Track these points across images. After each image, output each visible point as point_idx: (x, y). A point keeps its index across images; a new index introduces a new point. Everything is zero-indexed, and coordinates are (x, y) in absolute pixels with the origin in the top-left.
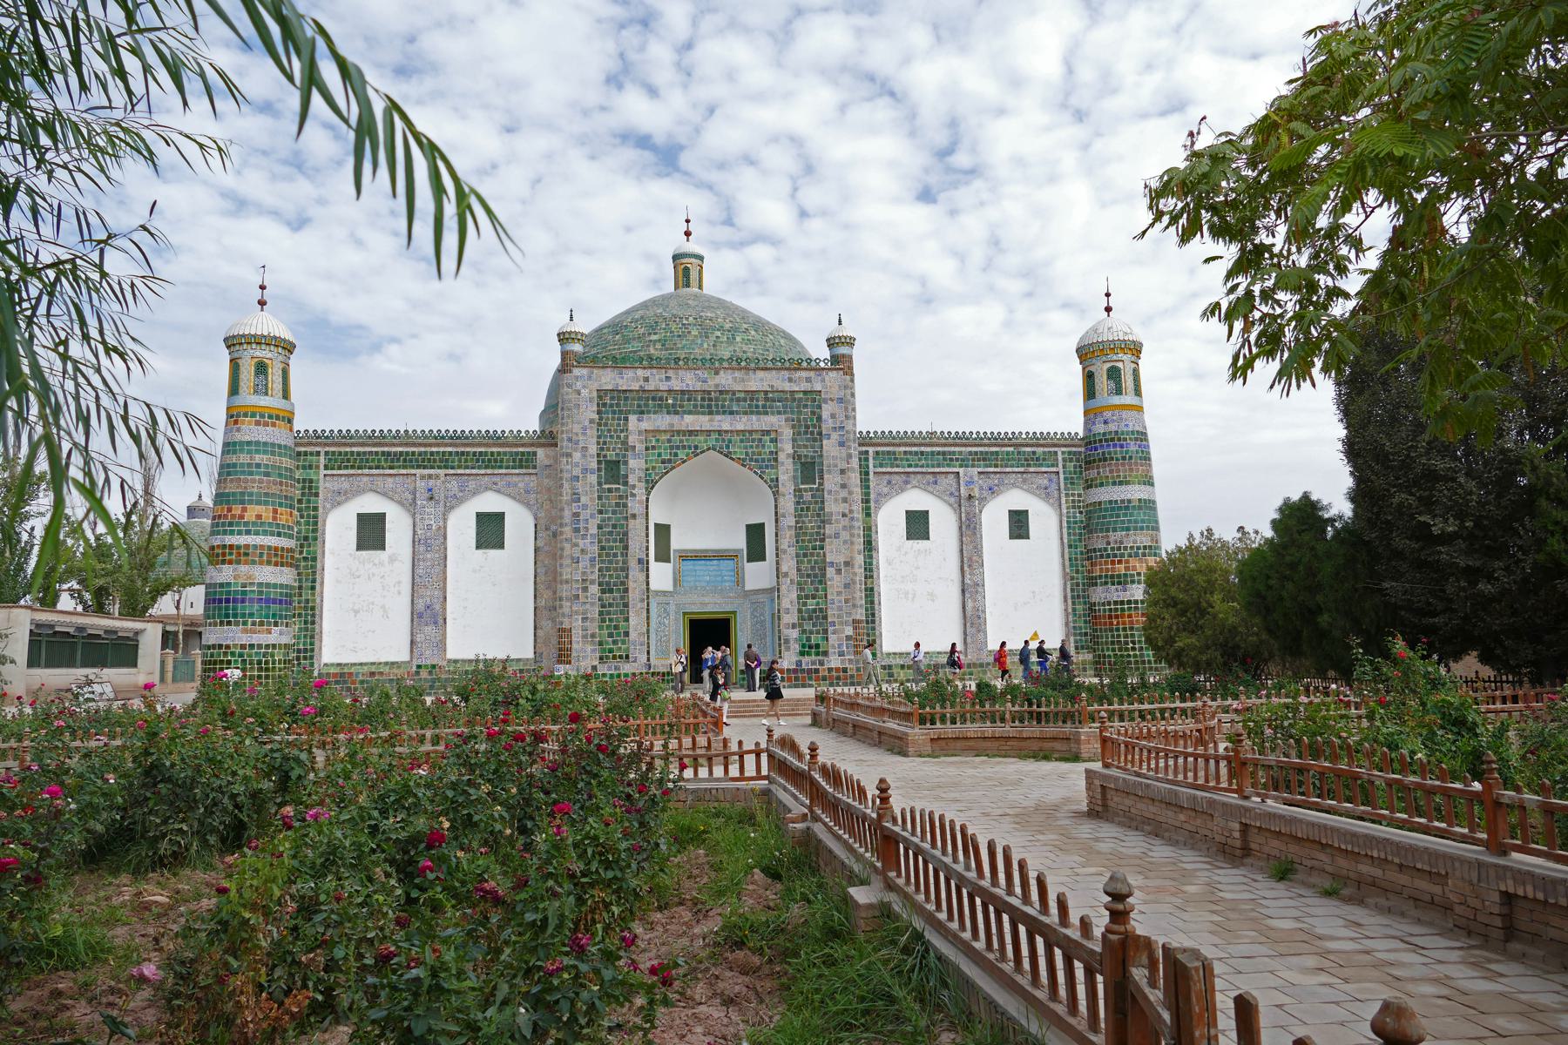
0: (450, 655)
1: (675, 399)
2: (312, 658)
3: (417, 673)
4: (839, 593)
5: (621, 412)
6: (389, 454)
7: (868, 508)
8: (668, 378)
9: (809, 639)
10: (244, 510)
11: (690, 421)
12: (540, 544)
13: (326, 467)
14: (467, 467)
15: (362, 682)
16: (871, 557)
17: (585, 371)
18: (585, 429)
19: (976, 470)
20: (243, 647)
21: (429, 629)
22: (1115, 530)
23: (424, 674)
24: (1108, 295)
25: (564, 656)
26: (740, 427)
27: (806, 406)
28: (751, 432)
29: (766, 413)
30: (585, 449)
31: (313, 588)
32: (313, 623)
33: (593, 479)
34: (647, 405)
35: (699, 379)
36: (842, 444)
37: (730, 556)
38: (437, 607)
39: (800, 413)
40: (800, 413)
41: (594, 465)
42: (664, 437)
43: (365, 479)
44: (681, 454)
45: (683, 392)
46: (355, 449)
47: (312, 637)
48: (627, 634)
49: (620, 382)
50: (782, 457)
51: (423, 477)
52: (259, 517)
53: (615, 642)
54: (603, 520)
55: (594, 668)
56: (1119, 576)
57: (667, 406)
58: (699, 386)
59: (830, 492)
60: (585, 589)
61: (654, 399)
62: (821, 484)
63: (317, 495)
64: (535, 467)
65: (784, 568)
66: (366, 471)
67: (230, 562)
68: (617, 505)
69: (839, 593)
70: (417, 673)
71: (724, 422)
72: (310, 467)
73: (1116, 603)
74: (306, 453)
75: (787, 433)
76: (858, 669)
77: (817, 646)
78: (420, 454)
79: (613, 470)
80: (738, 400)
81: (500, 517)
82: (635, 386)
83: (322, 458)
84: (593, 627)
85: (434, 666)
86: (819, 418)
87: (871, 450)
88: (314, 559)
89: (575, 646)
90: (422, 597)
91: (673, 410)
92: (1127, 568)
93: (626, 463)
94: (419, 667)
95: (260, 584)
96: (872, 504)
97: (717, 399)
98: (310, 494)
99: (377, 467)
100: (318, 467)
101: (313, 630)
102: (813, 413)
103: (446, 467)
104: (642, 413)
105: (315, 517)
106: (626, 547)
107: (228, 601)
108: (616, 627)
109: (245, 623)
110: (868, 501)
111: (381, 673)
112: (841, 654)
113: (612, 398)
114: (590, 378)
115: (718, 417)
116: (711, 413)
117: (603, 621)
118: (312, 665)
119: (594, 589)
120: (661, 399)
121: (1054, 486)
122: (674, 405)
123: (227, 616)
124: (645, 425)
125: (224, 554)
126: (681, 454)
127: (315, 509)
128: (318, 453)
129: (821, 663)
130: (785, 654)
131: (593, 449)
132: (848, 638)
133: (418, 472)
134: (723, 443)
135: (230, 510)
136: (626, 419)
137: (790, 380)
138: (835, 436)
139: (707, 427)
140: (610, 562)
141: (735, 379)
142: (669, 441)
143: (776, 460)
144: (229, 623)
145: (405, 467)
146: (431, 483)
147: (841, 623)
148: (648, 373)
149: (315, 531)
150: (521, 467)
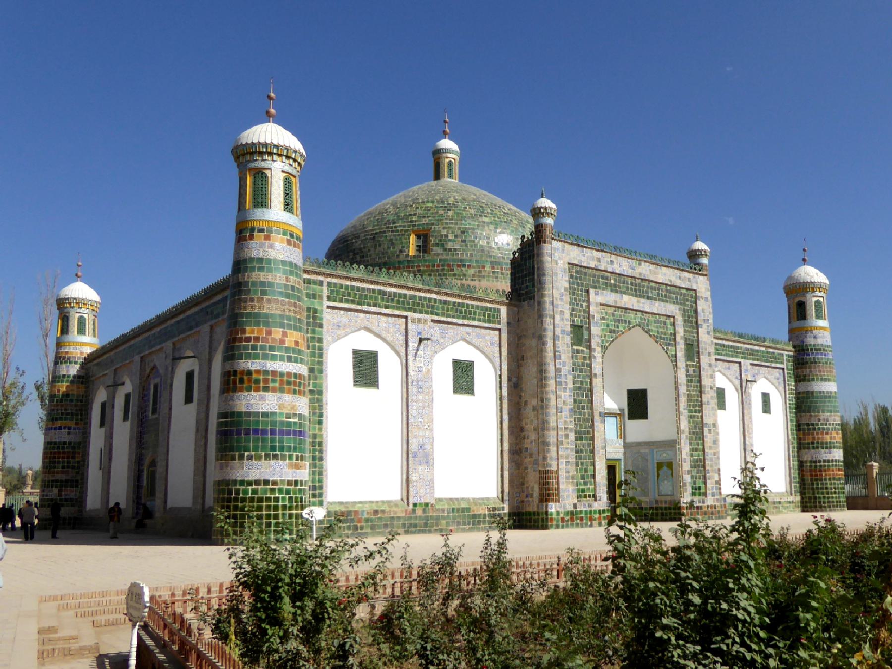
0: (438, 494)
3: (414, 511)
6: (384, 293)
10: (285, 334)
15: (367, 520)
19: (751, 362)
22: (823, 411)
23: (419, 512)
25: (547, 494)
38: (428, 447)
44: (621, 328)
51: (413, 321)
52: (297, 343)
53: (585, 483)
55: (575, 506)
56: (826, 443)
60: (567, 436)
66: (365, 308)
70: (414, 511)
73: (824, 461)
78: (411, 297)
79: (580, 334)
84: (572, 469)
85: (427, 504)
90: (416, 437)
92: (831, 438)
94: (415, 505)
99: (375, 305)
103: (432, 313)
107: (273, 432)
109: (290, 457)
111: (383, 512)
113: (577, 272)
117: (577, 465)
119: (572, 436)
133: (410, 314)
140: (580, 414)
145: (398, 308)
146: (421, 326)
148: (600, 254)
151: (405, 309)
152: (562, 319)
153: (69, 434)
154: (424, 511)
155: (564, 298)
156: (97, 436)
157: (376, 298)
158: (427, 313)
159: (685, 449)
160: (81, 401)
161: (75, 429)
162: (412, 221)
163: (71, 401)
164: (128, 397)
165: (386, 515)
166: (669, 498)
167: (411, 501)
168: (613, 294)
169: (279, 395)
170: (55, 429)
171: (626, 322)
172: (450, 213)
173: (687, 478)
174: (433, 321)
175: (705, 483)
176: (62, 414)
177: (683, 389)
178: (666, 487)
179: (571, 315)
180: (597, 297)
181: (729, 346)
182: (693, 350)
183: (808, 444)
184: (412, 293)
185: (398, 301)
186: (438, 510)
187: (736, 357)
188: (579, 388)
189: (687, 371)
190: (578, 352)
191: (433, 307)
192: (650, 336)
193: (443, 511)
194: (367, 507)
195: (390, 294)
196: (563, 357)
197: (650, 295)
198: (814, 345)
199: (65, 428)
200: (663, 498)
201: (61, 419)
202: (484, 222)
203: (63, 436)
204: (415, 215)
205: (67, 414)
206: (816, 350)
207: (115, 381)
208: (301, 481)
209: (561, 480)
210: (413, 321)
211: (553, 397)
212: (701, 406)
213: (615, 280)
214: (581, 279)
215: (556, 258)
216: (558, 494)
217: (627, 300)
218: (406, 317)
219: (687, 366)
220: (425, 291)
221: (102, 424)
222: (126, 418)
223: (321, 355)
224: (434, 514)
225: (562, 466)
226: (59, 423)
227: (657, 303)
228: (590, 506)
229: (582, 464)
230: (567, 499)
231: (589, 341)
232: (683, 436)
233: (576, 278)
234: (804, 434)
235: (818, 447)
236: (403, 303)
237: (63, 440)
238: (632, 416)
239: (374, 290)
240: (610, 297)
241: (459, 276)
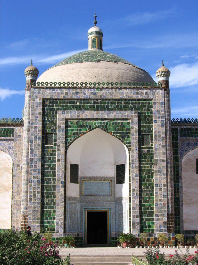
1: (80, 103)
5: (54, 109)
7: (177, 157)
8: (77, 93)
11: (88, 114)
12: (15, 174)
16: (178, 182)
18: (36, 117)
26: (113, 117)
27: (145, 106)
28: (117, 119)
29: (126, 110)
30: (36, 127)
34: (67, 106)
35: (92, 93)
37: (109, 180)
39: (142, 109)
40: (142, 109)
41: (40, 135)
42: (75, 121)
45: (84, 99)
48: (54, 218)
50: (132, 131)
57: (77, 106)
58: (92, 96)
59: (156, 149)
60: (35, 196)
61: (70, 103)
62: (152, 145)
64: (13, 136)
68: (51, 155)
71: (105, 114)
75: (136, 119)
76: (170, 239)
77: (149, 227)
80: (112, 103)
82: (61, 97)
86: (151, 113)
87: (179, 128)
91: (79, 108)
93: (56, 134)
96: (179, 156)
97: (101, 103)
102: (149, 110)
104: (64, 109)
106: (55, 176)
108: (50, 215)
110: (177, 154)
112: (161, 231)
114: (39, 93)
116: (98, 110)
120: (74, 103)
122: (80, 106)
126: (83, 130)
129: (151, 235)
132: (165, 223)
134: (104, 125)
136: (56, 113)
137: (137, 93)
139: (96, 116)
141: (110, 93)
142: (77, 123)
143: (129, 133)
147: (162, 215)
155: (38, 119)
171: (87, 126)
180: (61, 116)
192: (108, 132)
215: (34, 97)
227: (114, 112)
238: (117, 183)
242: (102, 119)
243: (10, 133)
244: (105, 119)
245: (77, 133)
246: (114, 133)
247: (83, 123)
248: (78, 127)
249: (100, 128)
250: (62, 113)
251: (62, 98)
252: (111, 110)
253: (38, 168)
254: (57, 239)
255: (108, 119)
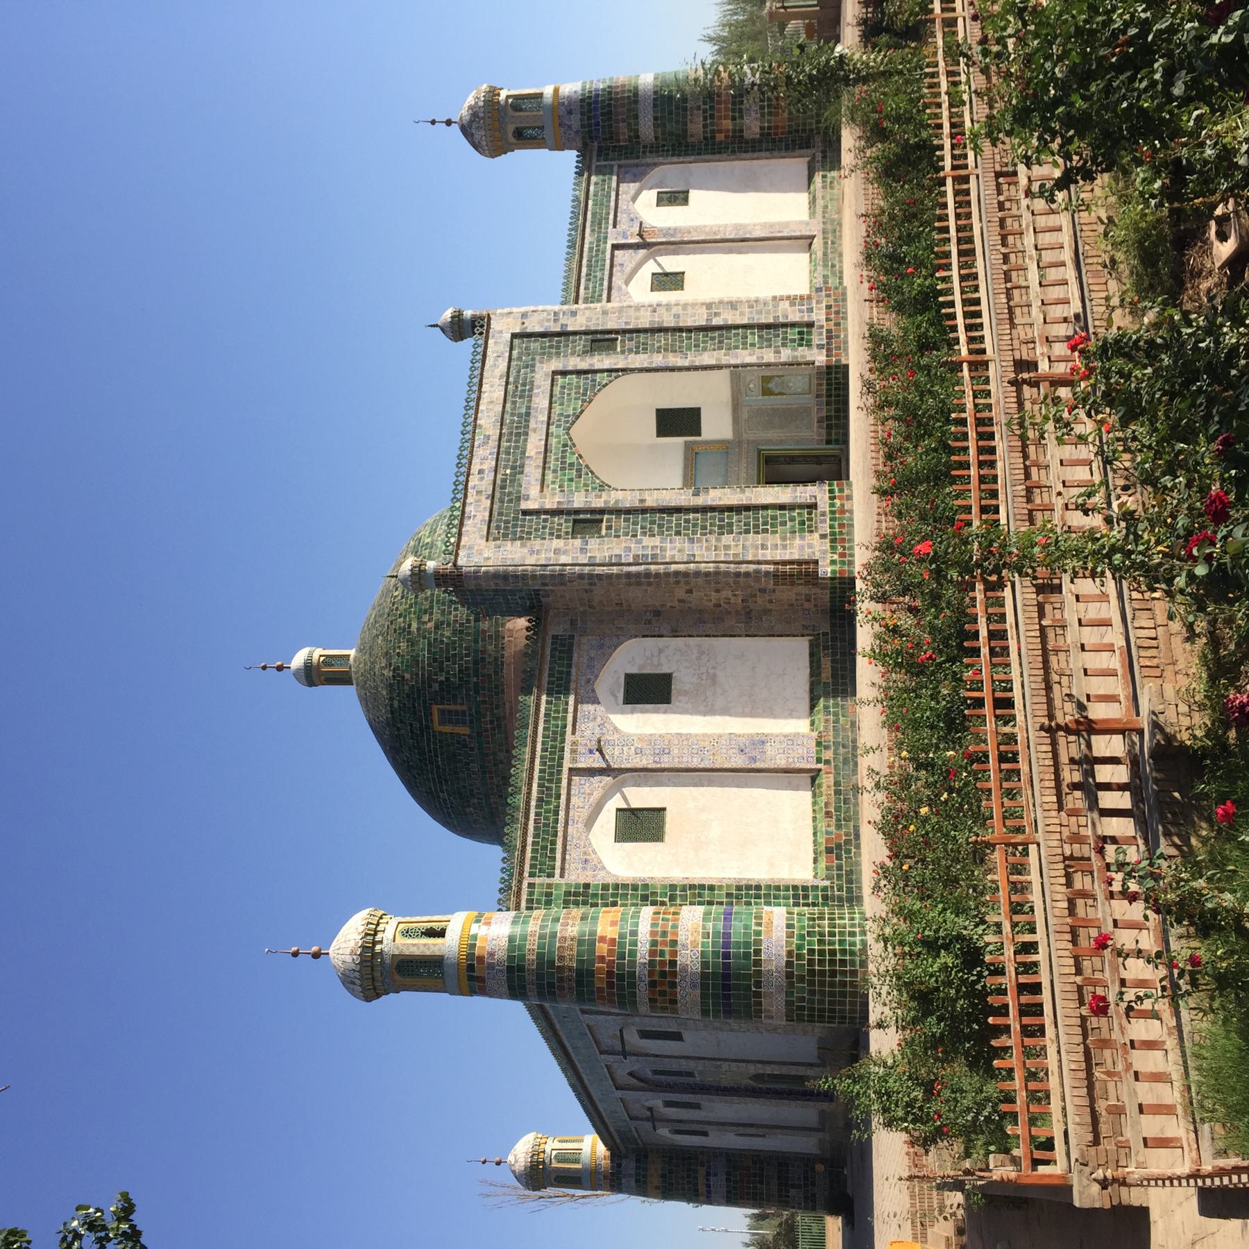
2: (805, 888)
3: (827, 762)
4: (742, 314)
5: (516, 519)
6: (540, 800)
8: (481, 472)
9: (794, 341)
13: (551, 875)
14: (566, 711)
15: (839, 827)
17: (461, 553)
20: (790, 935)
21: (770, 750)
23: (828, 755)
24: (433, 122)
25: (805, 572)
26: (546, 403)
31: (712, 888)
32: (758, 887)
33: (593, 543)
34: (510, 494)
35: (485, 443)
36: (574, 314)
41: (578, 542)
42: (550, 477)
43: (570, 829)
46: (530, 840)
47: (778, 888)
49: (479, 517)
50: (583, 365)
51: (574, 760)
54: (644, 534)
55: (823, 536)
57: (513, 475)
60: (727, 547)
61: (503, 487)
63: (587, 886)
65: (713, 362)
67: (674, 953)
69: (742, 314)
71: (538, 420)
72: (549, 895)
74: (530, 901)
78: (543, 763)
79: (586, 522)
80: (514, 409)
81: (630, 678)
83: (537, 880)
84: (771, 539)
85: (819, 744)
88: (673, 887)
89: (796, 557)
91: (518, 470)
94: (819, 761)
95: (704, 920)
98: (585, 894)
99: (556, 813)
100: (549, 886)
101: (768, 887)
103: (563, 734)
105: (616, 886)
111: (826, 804)
115: (532, 424)
117: (766, 531)
118: (815, 888)
119: (727, 539)
120: (504, 481)
121: (634, 170)
122: (513, 468)
123: (747, 955)
124: (534, 491)
125: (662, 963)
127: (605, 887)
128: (531, 885)
129: (822, 327)
130: (809, 359)
131: (556, 543)
133: (567, 764)
135: (602, 958)
138: (563, 320)
140: (695, 525)
142: (555, 471)
144: (758, 952)
145: (559, 781)
146: (581, 749)
149: (635, 887)
150: (570, 652)
151: (559, 772)
152: (565, 552)
153: (716, 1175)
154: (827, 748)
156: (716, 1140)
157: (547, 811)
158: (563, 741)
159: (746, 357)
160: (671, 1158)
161: (709, 1167)
162: (421, 729)
163: (671, 1172)
164: (668, 1104)
165: (833, 800)
166: (815, 382)
167: (813, 765)
168: (527, 470)
169: (679, 947)
170: (709, 1192)
172: (407, 676)
173: (786, 354)
174: (574, 733)
175: (793, 325)
176: (689, 1183)
177: (658, 360)
178: (798, 382)
179: (559, 537)
181: (589, 266)
182: (601, 340)
183: (734, 125)
184: (537, 761)
185: (550, 781)
186: (826, 728)
187: (604, 253)
188: (660, 526)
189: (630, 351)
190: (609, 528)
191: (555, 733)
193: (827, 721)
194: (822, 826)
195: (540, 792)
196: (617, 552)
197: (523, 410)
198: (582, 114)
199: (708, 1180)
200: (814, 388)
201: (696, 1185)
202: (418, 629)
203: (719, 1182)
204: (411, 725)
205: (689, 1176)
206: (589, 111)
207: (647, 1119)
208: (788, 919)
209: (787, 557)
210: (574, 760)
211: (673, 567)
212: (680, 330)
213: (506, 467)
214: (507, 522)
216: (807, 563)
217: (534, 444)
218: (570, 769)
219: (623, 352)
220: (534, 742)
221: (705, 1134)
222: (697, 1106)
223: (625, 886)
224: (831, 733)
225: (768, 555)
226: (702, 1189)
228: (823, 514)
229: (765, 523)
230: (810, 547)
231: (593, 511)
232: (725, 360)
233: (506, 528)
234: (720, 131)
235: (741, 111)
236: (551, 774)
237: (724, 1183)
239: (537, 814)
240: (532, 471)
241: (497, 665)
242: (548, 424)
243: (563, 645)
244: (549, 418)
245: (579, 470)
246: (584, 401)
247: (557, 460)
248: (563, 469)
249: (569, 428)
250: (527, 499)
251: (489, 502)
252: (529, 408)
253: (658, 544)
254: (832, 498)
255: (550, 413)
